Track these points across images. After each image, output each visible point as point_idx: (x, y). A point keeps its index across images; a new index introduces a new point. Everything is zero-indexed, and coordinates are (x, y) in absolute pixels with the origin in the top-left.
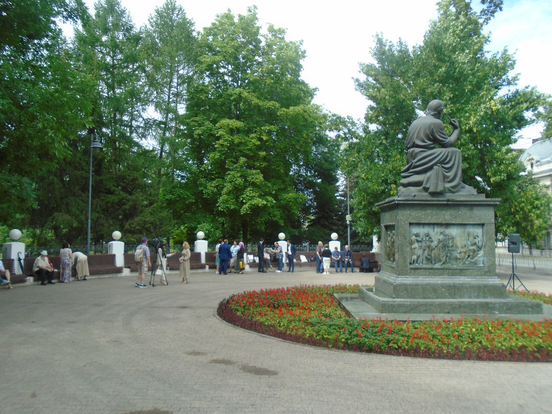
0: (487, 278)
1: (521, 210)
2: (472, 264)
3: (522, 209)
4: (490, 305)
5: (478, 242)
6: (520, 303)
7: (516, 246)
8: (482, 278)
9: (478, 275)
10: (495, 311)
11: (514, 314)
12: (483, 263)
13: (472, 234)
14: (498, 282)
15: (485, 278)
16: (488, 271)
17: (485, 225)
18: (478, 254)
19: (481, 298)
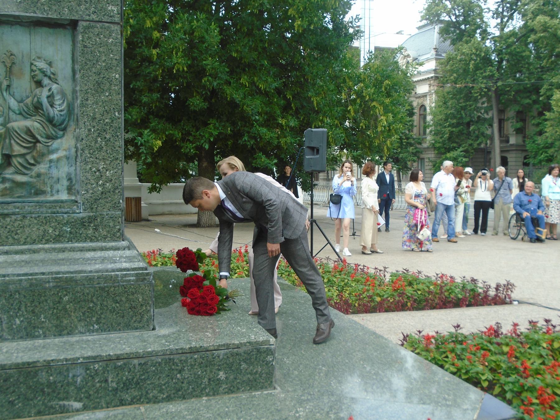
0: (82, 250)
2: (20, 192)
3: (359, 94)
4: (43, 377)
5: (51, 97)
6: (183, 352)
7: (318, 156)
8: (63, 250)
9: (44, 238)
10: (66, 398)
11: (156, 400)
12: (70, 190)
13: (27, 70)
15: (73, 250)
16: (91, 220)
17: (81, 24)
18: (52, 152)
19: (45, 337)
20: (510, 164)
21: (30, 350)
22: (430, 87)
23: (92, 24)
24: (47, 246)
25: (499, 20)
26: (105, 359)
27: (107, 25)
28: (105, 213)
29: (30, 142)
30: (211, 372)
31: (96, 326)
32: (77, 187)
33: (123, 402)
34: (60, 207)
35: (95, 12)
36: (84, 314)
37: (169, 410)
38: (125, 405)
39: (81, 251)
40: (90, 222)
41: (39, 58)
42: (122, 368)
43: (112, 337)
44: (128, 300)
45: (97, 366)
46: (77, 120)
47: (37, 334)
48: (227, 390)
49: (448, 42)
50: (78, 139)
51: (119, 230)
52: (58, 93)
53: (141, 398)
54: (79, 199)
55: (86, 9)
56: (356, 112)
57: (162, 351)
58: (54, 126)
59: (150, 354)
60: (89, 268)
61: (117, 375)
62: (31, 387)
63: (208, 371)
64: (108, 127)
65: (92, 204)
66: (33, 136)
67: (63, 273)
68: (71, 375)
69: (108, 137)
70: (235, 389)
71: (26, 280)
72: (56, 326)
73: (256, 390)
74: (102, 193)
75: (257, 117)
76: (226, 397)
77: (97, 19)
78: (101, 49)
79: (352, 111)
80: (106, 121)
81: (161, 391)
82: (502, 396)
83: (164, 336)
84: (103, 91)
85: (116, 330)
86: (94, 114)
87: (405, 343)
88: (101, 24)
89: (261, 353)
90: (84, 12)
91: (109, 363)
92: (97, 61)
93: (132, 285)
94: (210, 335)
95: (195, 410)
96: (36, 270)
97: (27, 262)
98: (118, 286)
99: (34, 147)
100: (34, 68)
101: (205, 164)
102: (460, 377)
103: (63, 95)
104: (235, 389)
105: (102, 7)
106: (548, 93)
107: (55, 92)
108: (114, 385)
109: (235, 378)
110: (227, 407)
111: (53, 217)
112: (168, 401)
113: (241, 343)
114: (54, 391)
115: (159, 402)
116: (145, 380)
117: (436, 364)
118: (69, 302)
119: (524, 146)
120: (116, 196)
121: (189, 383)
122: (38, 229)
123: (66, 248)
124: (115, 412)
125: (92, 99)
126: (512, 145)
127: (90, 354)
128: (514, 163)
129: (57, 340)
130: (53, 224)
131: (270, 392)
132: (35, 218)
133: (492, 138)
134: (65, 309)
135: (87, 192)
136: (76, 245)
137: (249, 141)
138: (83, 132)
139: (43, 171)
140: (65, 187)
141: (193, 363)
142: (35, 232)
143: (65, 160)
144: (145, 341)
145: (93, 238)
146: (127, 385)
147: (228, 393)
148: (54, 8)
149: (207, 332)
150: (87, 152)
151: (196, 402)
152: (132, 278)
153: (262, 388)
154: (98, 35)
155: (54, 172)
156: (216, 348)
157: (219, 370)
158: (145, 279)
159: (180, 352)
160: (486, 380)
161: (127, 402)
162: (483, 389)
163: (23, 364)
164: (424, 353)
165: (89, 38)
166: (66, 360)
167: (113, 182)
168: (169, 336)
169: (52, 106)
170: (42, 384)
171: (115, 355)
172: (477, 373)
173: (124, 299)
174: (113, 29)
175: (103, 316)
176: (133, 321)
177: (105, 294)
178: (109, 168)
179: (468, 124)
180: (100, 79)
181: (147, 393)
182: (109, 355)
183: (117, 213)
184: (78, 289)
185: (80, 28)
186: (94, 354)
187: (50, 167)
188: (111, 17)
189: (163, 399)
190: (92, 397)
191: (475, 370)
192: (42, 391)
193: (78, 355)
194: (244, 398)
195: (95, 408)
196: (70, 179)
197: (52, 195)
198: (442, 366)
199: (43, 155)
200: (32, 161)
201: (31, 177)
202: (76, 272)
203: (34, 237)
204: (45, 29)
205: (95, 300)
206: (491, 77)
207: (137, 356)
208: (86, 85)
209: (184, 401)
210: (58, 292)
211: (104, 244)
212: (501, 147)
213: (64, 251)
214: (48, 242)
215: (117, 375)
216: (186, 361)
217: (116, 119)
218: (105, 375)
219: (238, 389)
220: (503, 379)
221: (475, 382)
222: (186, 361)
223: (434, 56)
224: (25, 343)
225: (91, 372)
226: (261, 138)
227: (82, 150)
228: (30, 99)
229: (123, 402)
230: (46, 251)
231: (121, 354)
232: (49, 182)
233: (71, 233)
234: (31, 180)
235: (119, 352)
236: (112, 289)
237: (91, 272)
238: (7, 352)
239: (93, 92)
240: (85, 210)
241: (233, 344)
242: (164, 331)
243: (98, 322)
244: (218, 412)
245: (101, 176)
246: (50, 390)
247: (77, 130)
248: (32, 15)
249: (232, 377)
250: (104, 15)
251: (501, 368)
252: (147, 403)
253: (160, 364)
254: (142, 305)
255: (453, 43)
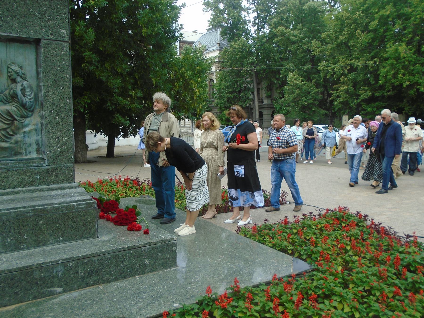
0: (48, 190)
1: (181, 77)
3: (182, 75)
4: (37, 274)
6: (124, 250)
8: (35, 191)
9: (22, 184)
10: (52, 286)
11: (108, 281)
12: (38, 151)
13: (5, 71)
14: (78, 198)
15: (42, 190)
16: (54, 170)
17: (43, 42)
19: (28, 248)
20: (264, 116)
21: (22, 258)
22: (216, 67)
23: (50, 42)
24: (24, 189)
25: (256, 28)
26: (76, 259)
27: (60, 42)
28: (62, 165)
29: (10, 120)
30: (141, 260)
31: (61, 239)
32: (42, 149)
33: (88, 284)
34: (33, 163)
35: (52, 34)
36: (53, 231)
37: (119, 286)
38: (89, 286)
39: (48, 190)
40: (53, 172)
41: (13, 63)
42: (87, 264)
43: (73, 245)
44: (81, 220)
45: (71, 264)
46: (42, 104)
47: (22, 247)
48: (150, 270)
49: (226, 40)
50: (42, 117)
51: (72, 175)
52: (28, 87)
53: (99, 281)
54: (45, 157)
55: (46, 31)
56: (180, 87)
57: (111, 250)
58: (26, 109)
59: (104, 253)
60: (55, 202)
61: (84, 268)
62: (29, 282)
63: (139, 260)
64: (63, 110)
65: (53, 160)
66: (12, 116)
67: (38, 206)
68: (55, 271)
69: (63, 116)
70: (155, 269)
71: (13, 212)
72: (35, 241)
73: (167, 268)
74: (60, 152)
75: (117, 90)
76: (150, 274)
77: (54, 39)
78: (57, 59)
79: (177, 86)
80: (62, 105)
81: (111, 275)
82: (300, 257)
83: (107, 241)
84: (59, 86)
85: (74, 240)
86: (53, 101)
87: (239, 232)
88: (56, 42)
89: (169, 246)
90: (45, 34)
91: (78, 261)
92: (54, 66)
93: (84, 210)
94: (136, 238)
95: (134, 284)
96: (19, 205)
97: (12, 201)
98: (75, 212)
99: (13, 123)
100: (11, 70)
101: (79, 120)
102: (275, 249)
103: (30, 87)
104: (155, 269)
105: (57, 31)
106: (285, 74)
107: (26, 86)
108: (82, 274)
109: (155, 263)
110: (153, 280)
111: (28, 170)
112: (116, 281)
113: (157, 241)
114: (44, 283)
115: (110, 282)
116: (101, 269)
117: (260, 243)
118: (43, 224)
119: (273, 105)
120: (69, 154)
121: (128, 269)
122: (18, 178)
123: (37, 189)
124: (85, 291)
125: (52, 91)
126: (265, 104)
127: (65, 257)
128: (266, 116)
129: (37, 250)
130: (28, 174)
131: (175, 268)
132: (16, 171)
133: (253, 100)
134: (40, 229)
135: (51, 152)
136: (44, 187)
137: (111, 106)
138: (47, 113)
139: (19, 139)
140: (35, 149)
141: (130, 256)
142: (16, 180)
143: (34, 131)
144: (97, 246)
145: (55, 182)
146: (90, 274)
147: (151, 272)
148: (24, 30)
149: (133, 236)
150: (49, 126)
151: (133, 279)
152: (83, 206)
153: (170, 267)
154: (54, 49)
155: (27, 140)
156: (143, 245)
157: (145, 259)
158: (92, 206)
159: (122, 250)
160: (290, 249)
161: (91, 284)
162: (288, 254)
163: (24, 267)
164: (252, 237)
165: (49, 51)
166: (52, 262)
167: (67, 145)
168: (110, 240)
169: (24, 96)
170: (36, 279)
171: (83, 256)
172: (286, 246)
173: (78, 220)
174: (64, 45)
175: (65, 232)
176: (84, 233)
177: (66, 218)
178: (64, 136)
179: (239, 92)
180: (57, 78)
181: (103, 277)
182: (79, 256)
183: (70, 165)
184: (49, 215)
185: (42, 44)
186: (68, 257)
187: (24, 136)
188: (63, 37)
189: (112, 280)
190: (68, 284)
191: (284, 244)
192: (37, 283)
193: (58, 258)
194: (161, 274)
195: (71, 290)
196: (38, 144)
197: (26, 155)
198: (263, 244)
199: (18, 129)
200: (11, 133)
201: (11, 143)
202: (46, 205)
203: (15, 183)
204: (17, 44)
205: (60, 222)
206: (252, 63)
207: (97, 255)
208: (47, 82)
209: (125, 280)
210: (36, 219)
211: (62, 185)
212: (259, 106)
213: (36, 192)
214: (25, 186)
215: (84, 268)
216: (126, 255)
217: (68, 104)
218: (77, 269)
219: (156, 269)
220: (300, 248)
221: (284, 251)
222: (126, 255)
223: (218, 48)
224: (16, 253)
225: (67, 268)
226: (119, 104)
227: (46, 125)
228: (8, 91)
229: (88, 284)
230: (24, 192)
231: (86, 255)
232: (24, 147)
233: (40, 179)
234: (11, 145)
235: (84, 254)
236: (71, 214)
237: (56, 204)
238: (7, 261)
239: (52, 86)
240: (49, 164)
241: (153, 242)
242: (105, 238)
243: (62, 236)
244: (149, 284)
245: (59, 141)
246: (42, 283)
247: (41, 112)
248: (9, 34)
249: (153, 262)
250: (58, 36)
251: (296, 242)
252: (103, 283)
253: (110, 258)
254: (90, 223)
255: (230, 40)
